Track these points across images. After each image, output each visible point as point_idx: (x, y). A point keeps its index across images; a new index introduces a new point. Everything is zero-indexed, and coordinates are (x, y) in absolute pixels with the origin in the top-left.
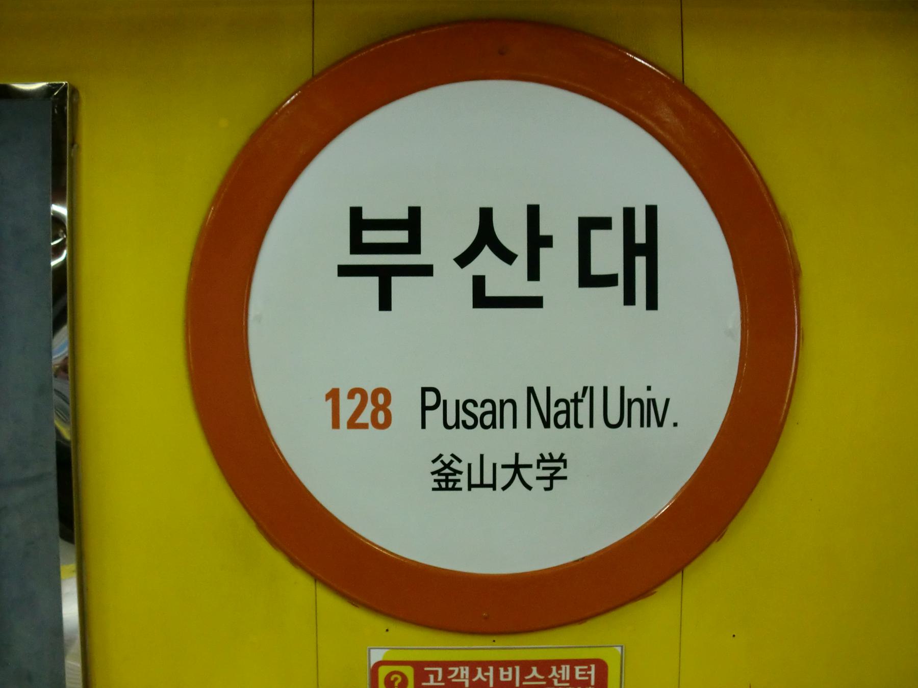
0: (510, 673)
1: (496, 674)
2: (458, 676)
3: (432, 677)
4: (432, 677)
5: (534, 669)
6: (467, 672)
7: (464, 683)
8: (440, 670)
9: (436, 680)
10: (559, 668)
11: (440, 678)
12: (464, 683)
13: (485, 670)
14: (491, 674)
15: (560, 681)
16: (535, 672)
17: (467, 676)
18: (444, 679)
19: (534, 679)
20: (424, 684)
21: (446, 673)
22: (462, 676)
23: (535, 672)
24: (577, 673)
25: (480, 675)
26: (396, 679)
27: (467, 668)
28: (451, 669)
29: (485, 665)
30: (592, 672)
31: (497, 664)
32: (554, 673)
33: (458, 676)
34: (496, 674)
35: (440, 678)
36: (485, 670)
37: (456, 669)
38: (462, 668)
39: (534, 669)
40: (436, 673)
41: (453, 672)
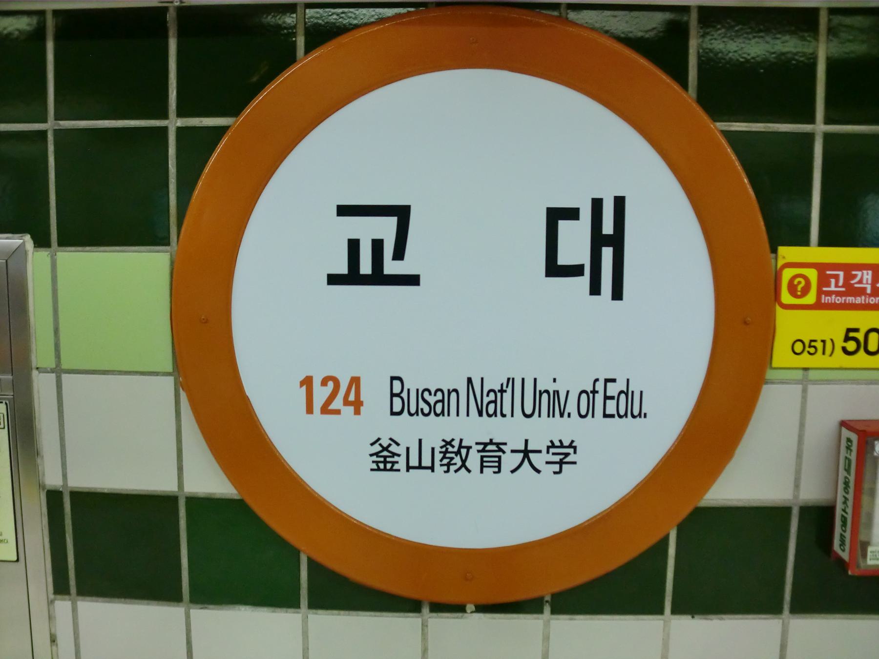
3: (833, 281)
4: (833, 281)
6: (870, 277)
7: (865, 289)
8: (841, 274)
9: (837, 286)
11: (841, 284)
12: (865, 289)
17: (870, 282)
18: (846, 283)
20: (825, 289)
21: (849, 277)
22: (865, 281)
26: (799, 283)
27: (870, 272)
28: (854, 273)
33: (860, 282)
35: (841, 284)
37: (859, 273)
38: (865, 272)
40: (836, 277)
41: (856, 276)
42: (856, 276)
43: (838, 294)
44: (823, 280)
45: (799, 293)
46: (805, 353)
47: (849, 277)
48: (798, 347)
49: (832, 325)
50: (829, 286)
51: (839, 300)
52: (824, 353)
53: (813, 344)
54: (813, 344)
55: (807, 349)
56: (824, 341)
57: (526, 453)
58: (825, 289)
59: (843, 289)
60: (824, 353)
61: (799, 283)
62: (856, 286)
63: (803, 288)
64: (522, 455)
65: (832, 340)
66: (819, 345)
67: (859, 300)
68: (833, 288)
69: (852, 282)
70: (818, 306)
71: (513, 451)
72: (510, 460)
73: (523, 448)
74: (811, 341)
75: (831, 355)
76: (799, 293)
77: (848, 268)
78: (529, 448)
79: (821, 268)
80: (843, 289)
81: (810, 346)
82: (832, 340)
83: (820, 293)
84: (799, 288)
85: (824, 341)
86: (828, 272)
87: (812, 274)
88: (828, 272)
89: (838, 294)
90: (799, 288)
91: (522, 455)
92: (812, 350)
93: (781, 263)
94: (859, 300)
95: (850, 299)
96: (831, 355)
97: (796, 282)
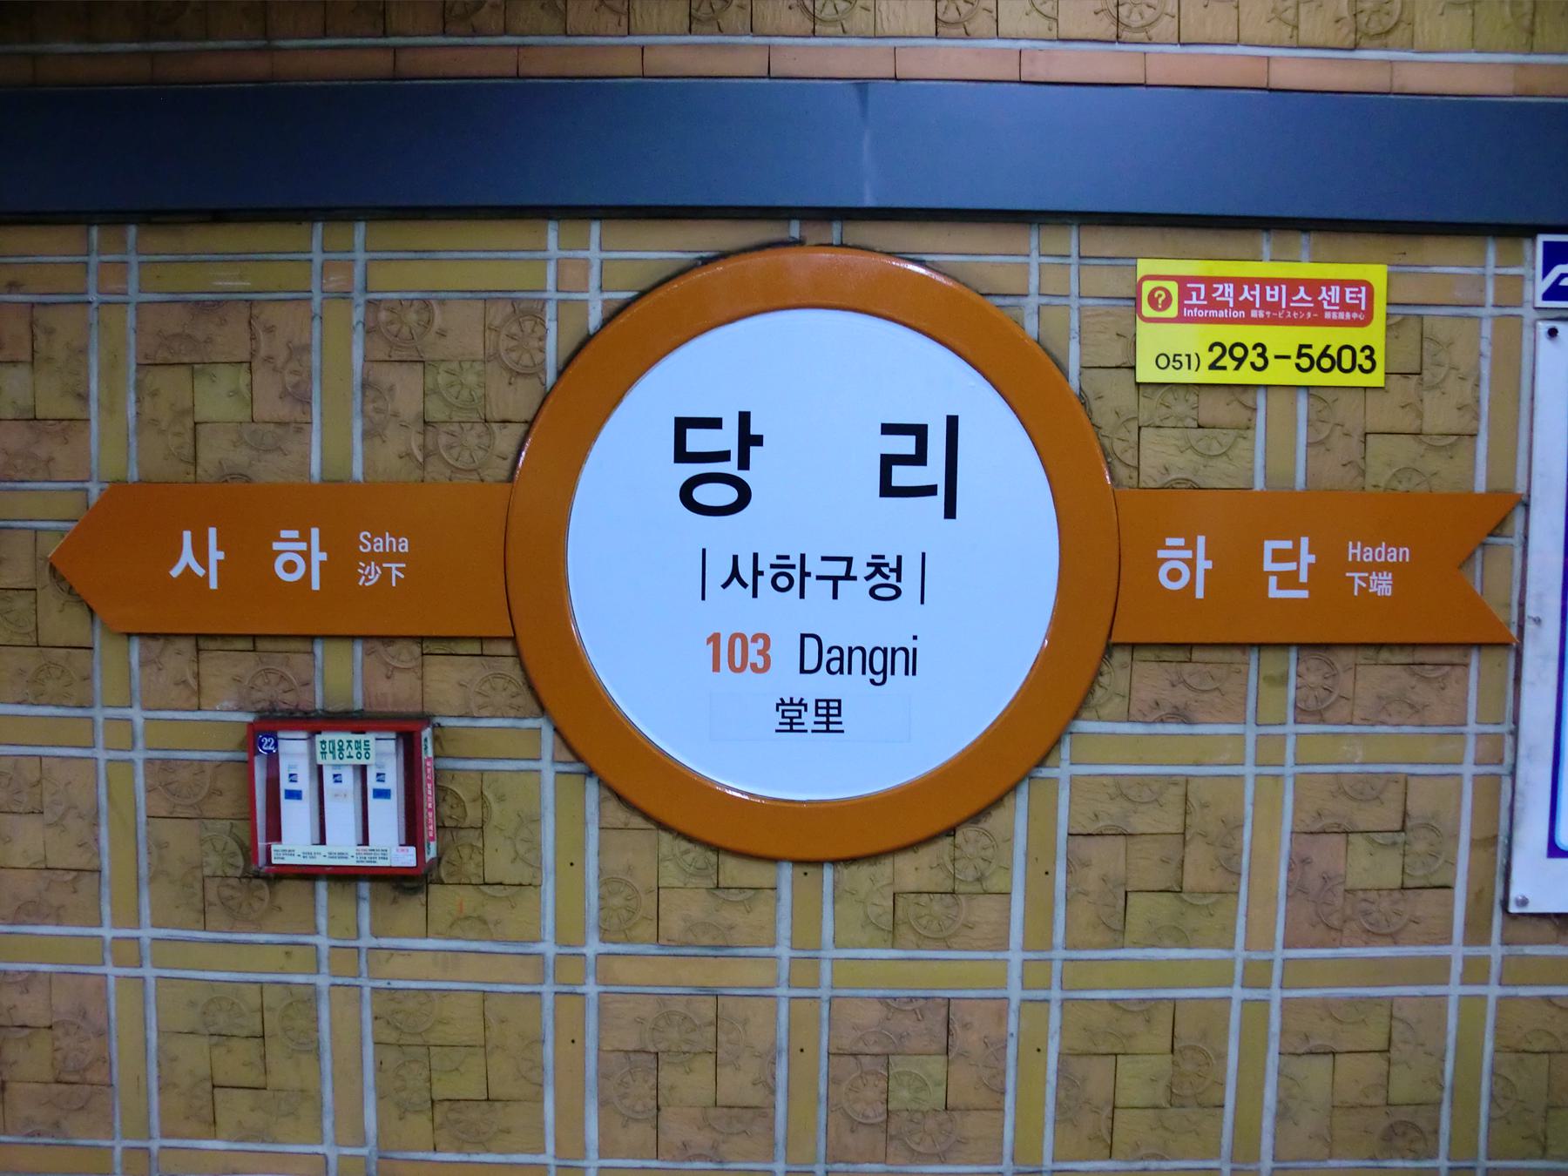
0: (1276, 293)
1: (1263, 293)
2: (1223, 295)
5: (1302, 289)
10: (1328, 290)
13: (1252, 288)
14: (1257, 293)
15: (1330, 303)
16: (1302, 294)
19: (1302, 300)
21: (1210, 290)
23: (1302, 294)
24: (1348, 296)
25: (1246, 294)
29: (1251, 282)
30: (1363, 296)
31: (1265, 282)
32: (1324, 295)
33: (1223, 295)
34: (1263, 293)
36: (1252, 288)
39: (1302, 289)
43: (1200, 307)
44: (1184, 294)
47: (1210, 290)
49: (1195, 339)
51: (1202, 313)
66: (1184, 360)
67: (1221, 314)
68: (1195, 301)
70: (1180, 319)
77: (1210, 281)
79: (1182, 281)
83: (1181, 306)
87: (1173, 287)
89: (1200, 307)
93: (1140, 275)
94: (1221, 314)
95: (1213, 313)
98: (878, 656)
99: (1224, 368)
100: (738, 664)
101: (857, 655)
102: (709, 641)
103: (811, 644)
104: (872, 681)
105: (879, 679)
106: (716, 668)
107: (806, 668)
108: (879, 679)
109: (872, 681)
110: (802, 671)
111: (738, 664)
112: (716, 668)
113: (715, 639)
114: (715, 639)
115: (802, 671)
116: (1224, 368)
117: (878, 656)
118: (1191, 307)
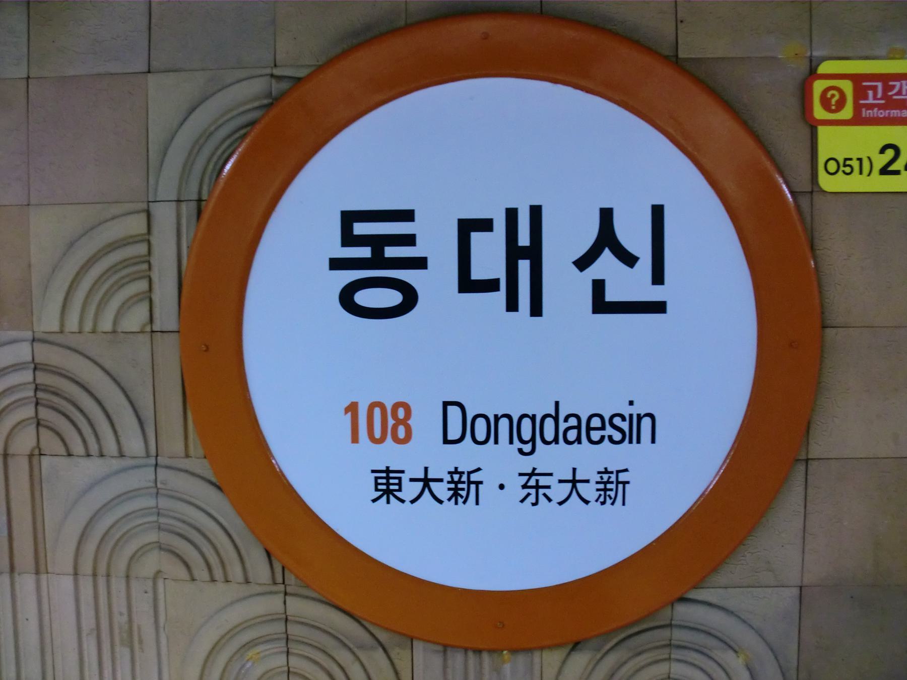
3: (870, 93)
4: (870, 93)
8: (880, 85)
9: (875, 98)
11: (879, 96)
20: (862, 102)
21: (887, 88)
35: (879, 96)
40: (874, 89)
42: (894, 86)
44: (860, 93)
45: (833, 108)
46: (840, 173)
47: (887, 88)
48: (832, 166)
50: (866, 98)
52: (861, 173)
53: (848, 162)
54: (848, 162)
55: (842, 168)
56: (860, 160)
57: (426, 482)
58: (862, 102)
59: (883, 102)
60: (861, 173)
61: (833, 96)
62: (895, 97)
63: (837, 102)
64: (421, 484)
65: (869, 158)
66: (855, 164)
68: (871, 101)
69: (890, 94)
71: (412, 480)
72: (410, 490)
73: (422, 476)
74: (846, 159)
75: (869, 175)
76: (833, 108)
77: (886, 79)
78: (430, 477)
79: (857, 79)
80: (883, 102)
81: (845, 166)
82: (869, 158)
84: (833, 101)
85: (860, 160)
86: (864, 84)
87: (847, 87)
88: (864, 84)
90: (833, 101)
91: (421, 484)
92: (848, 170)
96: (869, 175)
97: (829, 95)
98: (526, 424)
99: (897, 173)
100: (378, 434)
101: (504, 424)
102: (347, 410)
103: (454, 413)
104: (521, 451)
105: (527, 448)
106: (355, 439)
107: (450, 438)
108: (527, 448)
109: (521, 451)
110: (446, 441)
111: (378, 434)
112: (355, 439)
113: (352, 408)
114: (352, 408)
115: (446, 441)
116: (897, 173)
117: (526, 424)
118: (870, 107)
